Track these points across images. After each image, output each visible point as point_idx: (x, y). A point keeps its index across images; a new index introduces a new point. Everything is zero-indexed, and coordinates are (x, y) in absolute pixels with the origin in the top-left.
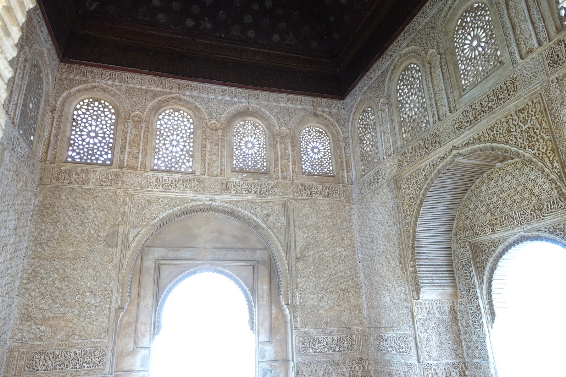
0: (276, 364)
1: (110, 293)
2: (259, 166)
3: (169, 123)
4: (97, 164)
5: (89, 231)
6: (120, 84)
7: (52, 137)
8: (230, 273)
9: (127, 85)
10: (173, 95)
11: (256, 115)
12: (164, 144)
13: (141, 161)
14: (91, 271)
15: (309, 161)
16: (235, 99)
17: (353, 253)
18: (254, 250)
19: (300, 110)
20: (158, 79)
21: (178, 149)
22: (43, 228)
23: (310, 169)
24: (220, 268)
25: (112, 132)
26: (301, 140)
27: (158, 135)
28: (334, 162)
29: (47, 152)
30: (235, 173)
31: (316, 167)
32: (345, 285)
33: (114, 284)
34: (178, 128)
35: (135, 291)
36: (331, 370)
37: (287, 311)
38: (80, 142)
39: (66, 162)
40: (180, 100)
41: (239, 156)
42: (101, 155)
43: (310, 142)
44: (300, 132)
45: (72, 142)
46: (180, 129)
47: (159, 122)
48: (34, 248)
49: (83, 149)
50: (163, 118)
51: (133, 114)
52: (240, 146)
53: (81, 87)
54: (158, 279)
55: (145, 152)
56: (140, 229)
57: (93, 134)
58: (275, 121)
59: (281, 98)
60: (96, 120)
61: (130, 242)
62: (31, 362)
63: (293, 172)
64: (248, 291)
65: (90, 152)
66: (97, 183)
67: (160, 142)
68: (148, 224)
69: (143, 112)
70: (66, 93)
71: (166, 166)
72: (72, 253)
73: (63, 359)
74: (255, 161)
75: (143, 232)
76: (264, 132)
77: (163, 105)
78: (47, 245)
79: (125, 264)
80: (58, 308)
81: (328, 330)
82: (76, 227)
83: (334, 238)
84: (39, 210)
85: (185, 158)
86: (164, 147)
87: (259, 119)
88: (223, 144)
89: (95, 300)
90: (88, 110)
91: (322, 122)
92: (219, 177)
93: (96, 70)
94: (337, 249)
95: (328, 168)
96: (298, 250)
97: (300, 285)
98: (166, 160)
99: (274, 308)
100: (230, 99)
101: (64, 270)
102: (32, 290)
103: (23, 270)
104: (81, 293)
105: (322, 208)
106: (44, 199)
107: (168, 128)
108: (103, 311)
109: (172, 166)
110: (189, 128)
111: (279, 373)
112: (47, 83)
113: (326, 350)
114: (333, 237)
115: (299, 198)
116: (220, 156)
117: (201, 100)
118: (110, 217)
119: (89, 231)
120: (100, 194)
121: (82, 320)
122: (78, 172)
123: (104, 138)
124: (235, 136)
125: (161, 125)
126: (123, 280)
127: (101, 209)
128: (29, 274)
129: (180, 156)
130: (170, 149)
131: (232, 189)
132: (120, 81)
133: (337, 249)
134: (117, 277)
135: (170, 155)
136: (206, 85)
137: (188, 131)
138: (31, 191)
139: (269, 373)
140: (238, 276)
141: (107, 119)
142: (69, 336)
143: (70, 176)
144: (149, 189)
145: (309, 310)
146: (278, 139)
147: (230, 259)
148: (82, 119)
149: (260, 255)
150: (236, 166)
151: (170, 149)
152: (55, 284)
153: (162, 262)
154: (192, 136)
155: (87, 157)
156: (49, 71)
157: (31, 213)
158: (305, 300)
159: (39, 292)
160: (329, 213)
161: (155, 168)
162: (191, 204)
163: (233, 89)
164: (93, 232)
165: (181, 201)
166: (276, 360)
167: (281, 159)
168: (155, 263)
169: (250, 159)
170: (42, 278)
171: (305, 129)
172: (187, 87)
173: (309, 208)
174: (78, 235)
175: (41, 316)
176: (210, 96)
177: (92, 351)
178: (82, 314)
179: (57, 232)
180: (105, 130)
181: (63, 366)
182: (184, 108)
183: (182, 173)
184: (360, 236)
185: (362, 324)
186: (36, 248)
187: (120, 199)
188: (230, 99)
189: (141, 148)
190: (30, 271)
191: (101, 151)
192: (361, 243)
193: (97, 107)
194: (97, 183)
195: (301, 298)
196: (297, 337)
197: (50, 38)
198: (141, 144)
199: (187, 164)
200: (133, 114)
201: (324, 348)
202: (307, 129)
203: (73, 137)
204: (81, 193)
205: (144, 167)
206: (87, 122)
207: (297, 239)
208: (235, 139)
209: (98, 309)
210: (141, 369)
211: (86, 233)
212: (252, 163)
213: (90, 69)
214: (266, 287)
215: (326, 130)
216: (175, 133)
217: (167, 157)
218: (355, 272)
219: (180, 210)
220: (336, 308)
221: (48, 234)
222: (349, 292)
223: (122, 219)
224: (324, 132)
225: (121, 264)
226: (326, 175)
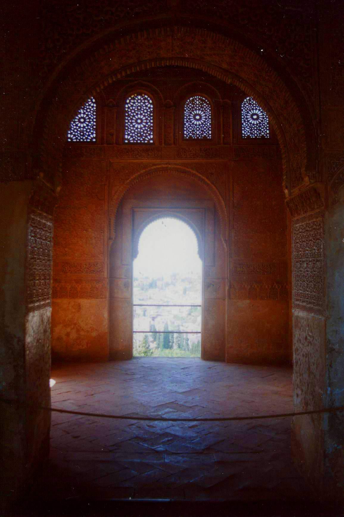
12: (132, 123)
23: (248, 134)
25: (95, 117)
27: (126, 116)
34: (141, 108)
37: (225, 245)
41: (189, 127)
42: (89, 135)
43: (250, 110)
47: (127, 106)
50: (130, 101)
52: (189, 119)
57: (82, 120)
65: (82, 134)
67: (129, 122)
71: (134, 140)
74: (202, 130)
76: (210, 104)
86: (131, 125)
98: (134, 135)
107: (134, 110)
109: (138, 140)
110: (150, 108)
123: (89, 122)
124: (185, 110)
125: (129, 108)
129: (144, 130)
130: (136, 126)
137: (149, 110)
150: (187, 135)
151: (136, 126)
154: (152, 114)
161: (126, 141)
162: (153, 168)
180: (90, 116)
191: (88, 132)
199: (149, 137)
216: (139, 113)
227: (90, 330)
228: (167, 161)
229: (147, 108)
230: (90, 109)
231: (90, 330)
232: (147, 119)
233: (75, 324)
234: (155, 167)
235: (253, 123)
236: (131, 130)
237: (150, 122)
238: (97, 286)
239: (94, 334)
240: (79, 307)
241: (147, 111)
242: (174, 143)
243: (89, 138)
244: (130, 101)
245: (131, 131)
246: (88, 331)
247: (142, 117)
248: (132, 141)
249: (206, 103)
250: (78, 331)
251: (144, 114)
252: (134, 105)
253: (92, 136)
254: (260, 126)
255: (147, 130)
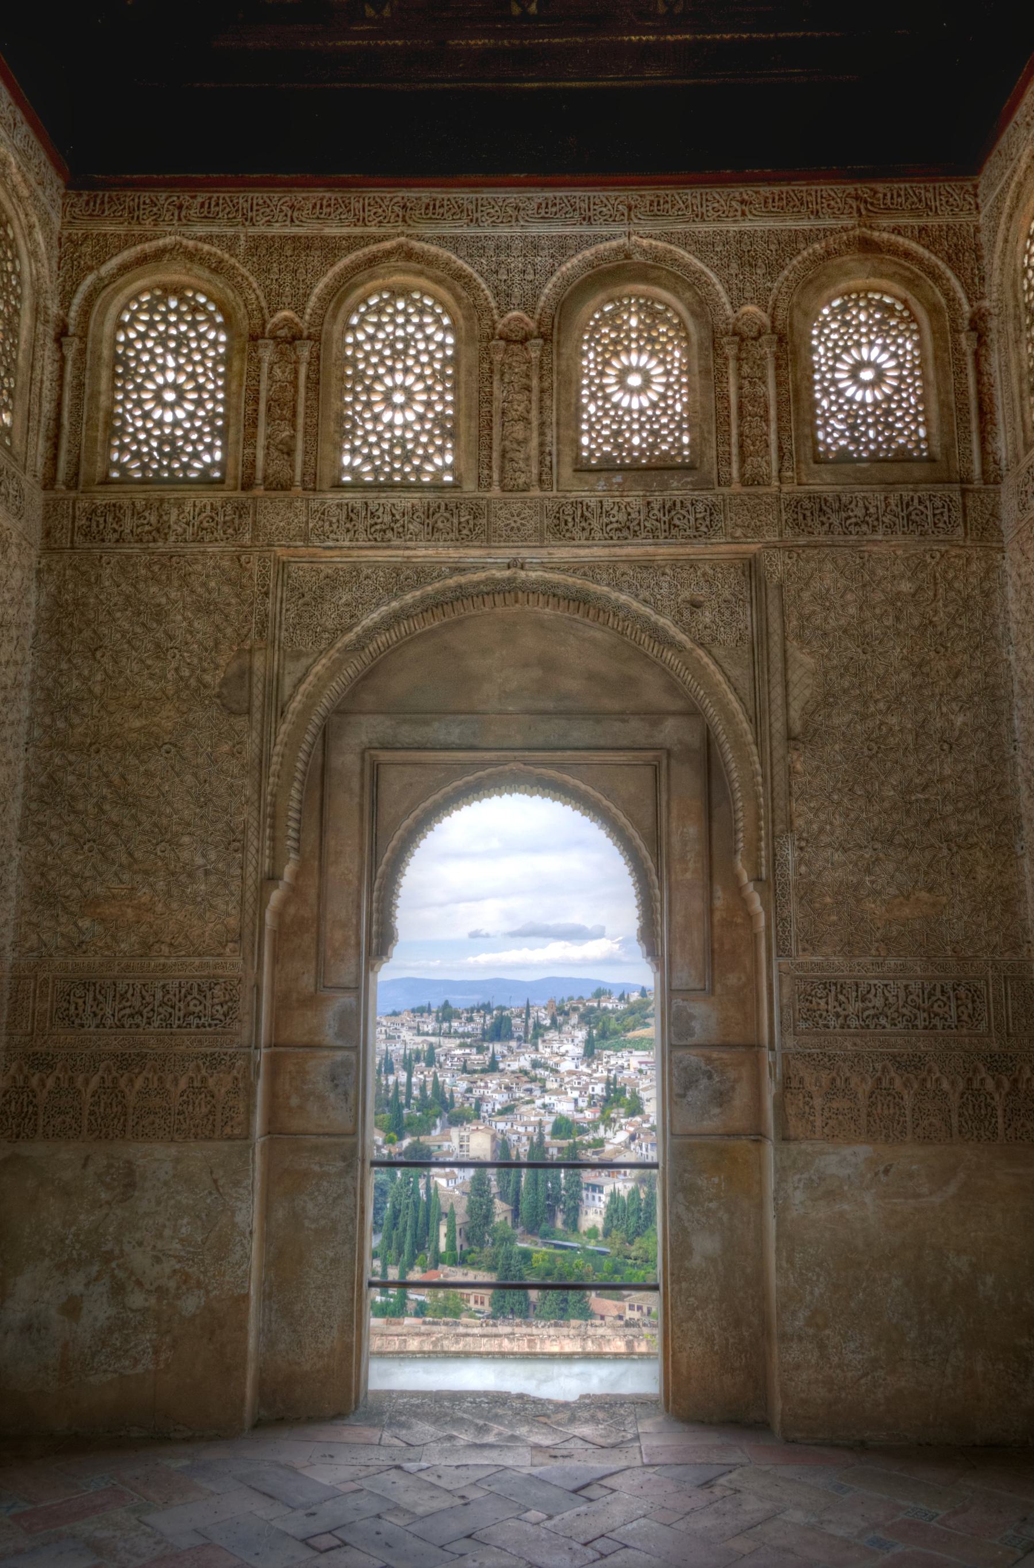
0: (725, 1056)
1: (240, 837)
2: (664, 447)
3: (381, 335)
4: (187, 481)
5: (177, 670)
6: (230, 231)
7: (66, 414)
8: (583, 787)
9: (252, 231)
10: (388, 245)
11: (656, 273)
13: (305, 463)
14: (189, 778)
15: (841, 416)
16: (585, 230)
17: (993, 718)
18: (654, 716)
19: (809, 238)
20: (339, 195)
21: (411, 416)
22: (64, 666)
23: (842, 442)
24: (552, 773)
26: (815, 343)
28: (934, 407)
29: (55, 458)
30: (586, 476)
31: (865, 434)
32: (959, 823)
33: (248, 815)
34: (407, 347)
35: (313, 836)
36: (898, 1082)
38: (139, 424)
39: (107, 481)
40: (410, 255)
41: (599, 420)
43: (846, 349)
44: (810, 315)
45: (118, 424)
46: (412, 352)
48: (47, 720)
49: (147, 442)
50: (363, 321)
51: (275, 320)
53: (127, 255)
54: (375, 802)
55: (313, 433)
56: (311, 660)
57: (170, 396)
58: (719, 287)
59: (743, 202)
60: (176, 353)
61: (286, 698)
62: (65, 1005)
63: (781, 458)
64: (639, 842)
65: (167, 449)
66: (188, 536)
67: (356, 399)
68: (331, 644)
69: (300, 311)
70: (90, 279)
71: (376, 471)
72: (139, 730)
73: (137, 1003)
74: (653, 433)
75: (318, 668)
77: (359, 278)
78: (76, 710)
79: (275, 759)
80: (116, 874)
81: (892, 962)
82: (142, 661)
83: (926, 669)
84: (50, 619)
85: (431, 442)
87: (665, 287)
88: (546, 384)
89: (204, 856)
90: (151, 325)
91: (893, 269)
92: (536, 492)
93: (164, 195)
94: (932, 707)
95: (913, 432)
96: (795, 714)
97: (799, 822)
99: (719, 892)
100: (568, 230)
101: (122, 776)
102: (52, 828)
103: (27, 778)
104: (168, 836)
105: (880, 572)
106: (59, 589)
107: (379, 353)
108: (226, 885)
109: (394, 470)
110: (442, 346)
111: (736, 1081)
112: (33, 254)
113: (883, 1021)
114: (920, 666)
115: (802, 540)
116: (535, 423)
117: (474, 248)
118: (229, 631)
119: (177, 670)
120: (199, 567)
121: (175, 906)
122: (139, 506)
123: (199, 403)
124: (584, 355)
125: (357, 345)
126: (274, 805)
127: (204, 608)
128: (43, 786)
129: (417, 435)
130: (387, 417)
131: (578, 528)
132: (231, 222)
133: (932, 707)
134: (256, 797)
135: (388, 435)
136: (487, 194)
137: (439, 355)
138: (23, 567)
139: (704, 1082)
140: (608, 797)
141: (205, 345)
142: (147, 948)
143: (119, 521)
144: (330, 544)
145: (828, 900)
146: (730, 351)
147: (580, 744)
148: (139, 352)
149: (671, 731)
150: (592, 453)
151: (387, 417)
152: (103, 812)
153: (385, 756)
155: (159, 462)
156: (34, 219)
157: (33, 629)
158: (819, 865)
159: (70, 834)
160: (906, 587)
161: (347, 478)
162: (451, 582)
163: (578, 193)
164: (186, 673)
165: (422, 574)
166: (725, 1045)
167: (741, 416)
168: (363, 759)
169: (636, 426)
170: (73, 798)
171: (829, 302)
172: (432, 212)
173: (836, 574)
174: (150, 683)
175: (77, 892)
176: (504, 231)
177: (205, 987)
178: (175, 892)
179: (99, 677)
180: (201, 380)
181: (138, 1019)
182: (423, 282)
183: (420, 487)
184: (1018, 659)
185: (1015, 947)
186: (53, 720)
187: (251, 577)
188: (568, 230)
189: (300, 421)
190: (43, 779)
191: (194, 443)
192: (1021, 682)
193: (176, 311)
194: (188, 536)
195: (801, 861)
196: (787, 980)
197: (19, 116)
198: (301, 409)
199: (438, 461)
200: (275, 320)
201: (876, 1016)
202: (836, 303)
203: (120, 411)
204: (148, 566)
205: (312, 484)
206: (152, 360)
207: (794, 677)
208: (589, 362)
209: (213, 879)
210: (339, 1043)
211: (169, 676)
212: (643, 440)
213: (146, 196)
214: (693, 830)
215: (910, 297)
216: (399, 366)
217: (378, 445)
218: (999, 778)
219: (423, 599)
220: (924, 895)
221: (76, 684)
222: (972, 846)
223: (260, 633)
224: (899, 307)
225: (262, 762)
226: (902, 457)
227: (172, 1284)
228: (512, 553)
229: (432, 347)
230: (203, 352)
231: (172, 1284)
232: (429, 389)
233: (107, 1258)
234: (463, 580)
235: (858, 397)
236: (367, 433)
237: (442, 398)
238: (211, 1082)
239: (191, 1304)
240: (128, 1181)
241: (432, 358)
242: (541, 481)
243: (197, 465)
244: (363, 321)
245: (364, 438)
246: (161, 1292)
247: (410, 380)
248: (368, 479)
249: (667, 321)
250: (118, 1290)
251: (417, 370)
252: (381, 335)
253: (207, 458)
254: (889, 412)
255: (430, 433)
